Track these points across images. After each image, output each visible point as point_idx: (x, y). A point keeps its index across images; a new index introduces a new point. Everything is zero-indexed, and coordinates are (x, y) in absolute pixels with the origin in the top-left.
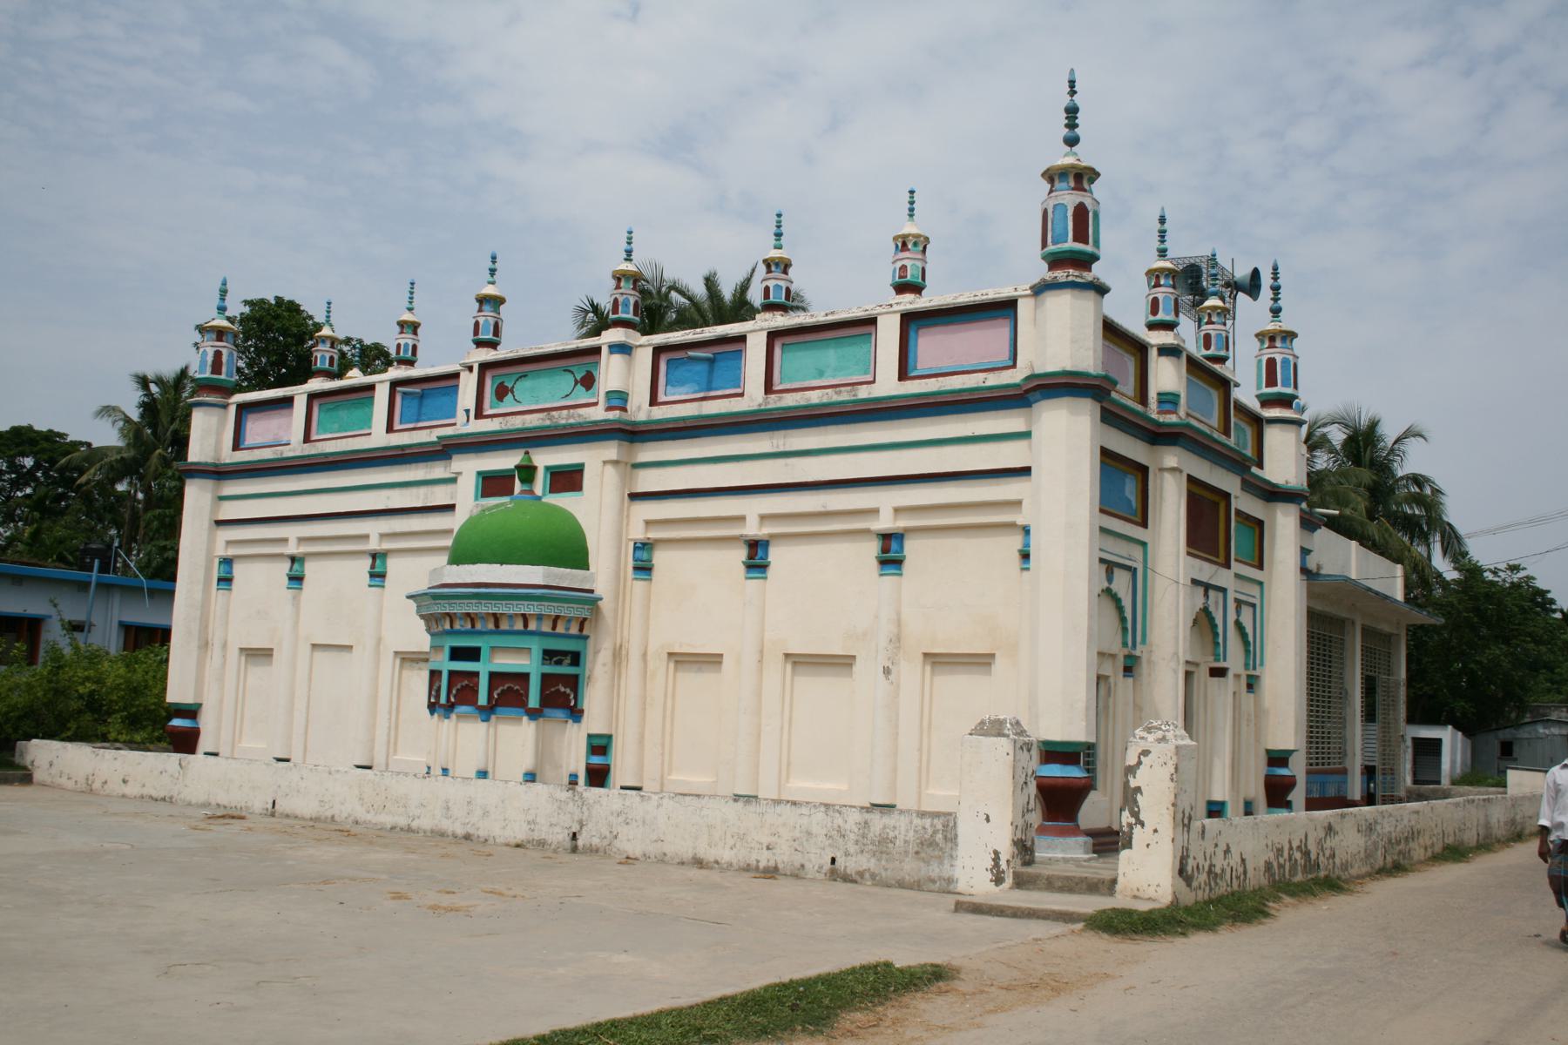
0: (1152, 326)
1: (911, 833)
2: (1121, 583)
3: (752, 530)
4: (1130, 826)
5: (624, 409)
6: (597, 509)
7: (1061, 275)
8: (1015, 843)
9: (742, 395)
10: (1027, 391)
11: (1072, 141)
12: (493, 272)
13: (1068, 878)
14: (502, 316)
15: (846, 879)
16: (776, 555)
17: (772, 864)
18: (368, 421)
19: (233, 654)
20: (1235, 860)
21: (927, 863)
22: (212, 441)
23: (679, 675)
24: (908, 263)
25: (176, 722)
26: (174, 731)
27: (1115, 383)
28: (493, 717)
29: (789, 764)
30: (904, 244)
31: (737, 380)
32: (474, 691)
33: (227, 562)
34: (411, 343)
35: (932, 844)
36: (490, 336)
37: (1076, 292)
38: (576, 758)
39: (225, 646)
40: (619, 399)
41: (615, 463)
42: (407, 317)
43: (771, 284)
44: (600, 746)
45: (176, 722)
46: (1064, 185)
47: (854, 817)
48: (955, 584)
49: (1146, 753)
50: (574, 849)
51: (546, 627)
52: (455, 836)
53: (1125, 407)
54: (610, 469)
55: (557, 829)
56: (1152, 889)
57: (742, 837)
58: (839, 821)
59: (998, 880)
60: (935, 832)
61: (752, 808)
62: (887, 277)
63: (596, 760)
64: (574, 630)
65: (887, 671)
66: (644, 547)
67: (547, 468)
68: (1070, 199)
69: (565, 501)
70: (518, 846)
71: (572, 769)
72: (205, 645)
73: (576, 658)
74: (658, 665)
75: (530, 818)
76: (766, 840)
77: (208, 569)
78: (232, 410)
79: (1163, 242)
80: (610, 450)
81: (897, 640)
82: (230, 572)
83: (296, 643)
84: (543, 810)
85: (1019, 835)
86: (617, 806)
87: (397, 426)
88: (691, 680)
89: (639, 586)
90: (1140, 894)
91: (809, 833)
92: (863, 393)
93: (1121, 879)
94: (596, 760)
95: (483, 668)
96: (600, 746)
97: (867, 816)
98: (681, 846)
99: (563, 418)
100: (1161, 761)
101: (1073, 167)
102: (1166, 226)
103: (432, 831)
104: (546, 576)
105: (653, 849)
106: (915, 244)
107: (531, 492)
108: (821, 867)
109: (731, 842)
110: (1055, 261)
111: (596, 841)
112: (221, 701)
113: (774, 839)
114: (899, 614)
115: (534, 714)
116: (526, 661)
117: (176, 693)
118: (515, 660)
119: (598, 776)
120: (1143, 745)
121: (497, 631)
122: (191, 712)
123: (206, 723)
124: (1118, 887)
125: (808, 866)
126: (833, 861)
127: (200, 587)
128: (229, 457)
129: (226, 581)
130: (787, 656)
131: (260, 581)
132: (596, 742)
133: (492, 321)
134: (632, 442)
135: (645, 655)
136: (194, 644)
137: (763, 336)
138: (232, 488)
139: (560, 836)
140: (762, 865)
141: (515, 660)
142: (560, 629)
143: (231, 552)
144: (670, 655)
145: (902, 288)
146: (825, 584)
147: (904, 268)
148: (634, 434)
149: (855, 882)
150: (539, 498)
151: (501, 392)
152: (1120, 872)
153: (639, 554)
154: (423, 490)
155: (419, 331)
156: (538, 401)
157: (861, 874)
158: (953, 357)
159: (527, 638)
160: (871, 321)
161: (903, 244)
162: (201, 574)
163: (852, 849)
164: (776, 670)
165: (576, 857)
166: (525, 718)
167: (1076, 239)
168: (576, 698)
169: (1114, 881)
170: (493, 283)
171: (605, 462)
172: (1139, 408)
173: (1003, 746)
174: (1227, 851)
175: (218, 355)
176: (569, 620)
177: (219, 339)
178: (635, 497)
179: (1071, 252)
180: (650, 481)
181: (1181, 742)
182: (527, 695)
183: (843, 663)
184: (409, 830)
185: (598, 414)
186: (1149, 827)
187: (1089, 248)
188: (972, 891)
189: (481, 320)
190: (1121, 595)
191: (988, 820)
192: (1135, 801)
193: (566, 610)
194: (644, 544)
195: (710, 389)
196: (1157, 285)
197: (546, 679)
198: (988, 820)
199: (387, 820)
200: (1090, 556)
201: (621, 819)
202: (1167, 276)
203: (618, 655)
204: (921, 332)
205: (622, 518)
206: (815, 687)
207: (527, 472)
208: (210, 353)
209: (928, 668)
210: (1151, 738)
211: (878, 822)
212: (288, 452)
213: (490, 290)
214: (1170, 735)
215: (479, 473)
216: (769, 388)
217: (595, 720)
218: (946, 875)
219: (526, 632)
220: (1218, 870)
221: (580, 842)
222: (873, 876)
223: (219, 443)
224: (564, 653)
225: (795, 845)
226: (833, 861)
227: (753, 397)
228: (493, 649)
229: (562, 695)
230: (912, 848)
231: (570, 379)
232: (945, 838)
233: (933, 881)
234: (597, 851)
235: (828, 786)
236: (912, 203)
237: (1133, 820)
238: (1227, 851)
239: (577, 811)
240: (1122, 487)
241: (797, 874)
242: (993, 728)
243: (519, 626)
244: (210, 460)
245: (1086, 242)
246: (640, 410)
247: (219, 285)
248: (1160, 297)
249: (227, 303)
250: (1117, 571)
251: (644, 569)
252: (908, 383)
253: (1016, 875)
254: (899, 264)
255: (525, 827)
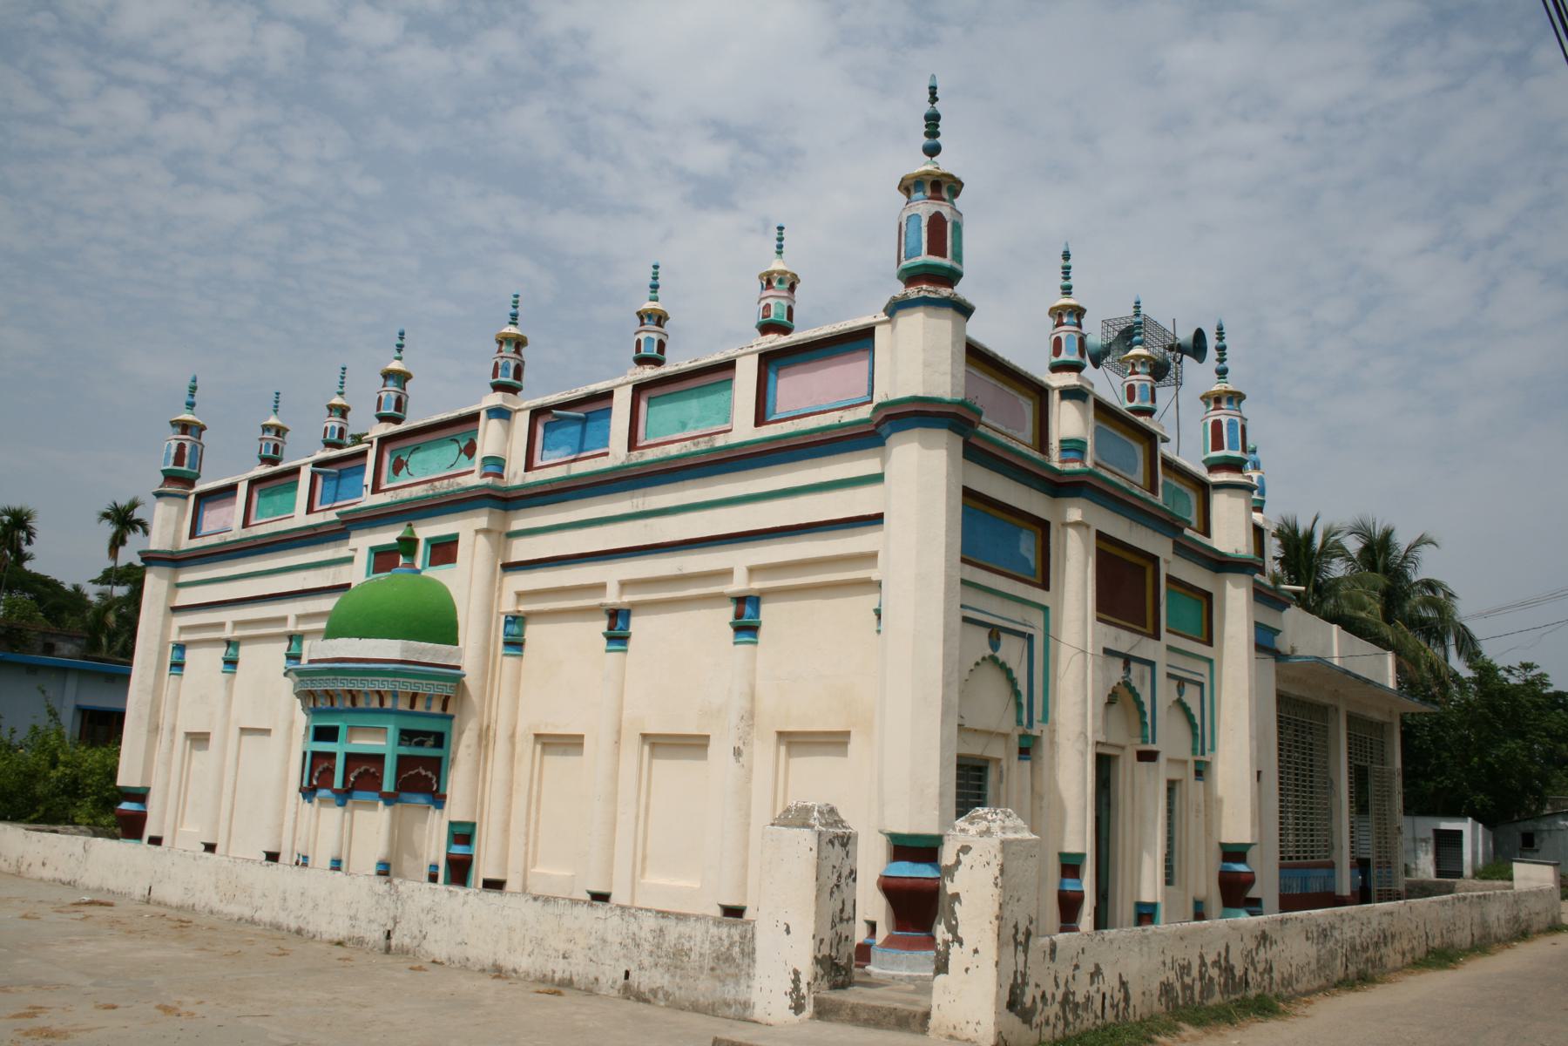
0: (1055, 368)
1: (707, 945)
2: (1011, 652)
3: (612, 598)
4: (946, 944)
5: (501, 476)
6: (467, 583)
7: (913, 293)
8: (817, 961)
9: (606, 454)
10: (877, 425)
11: (932, 151)
12: (400, 348)
13: (874, 1009)
14: (408, 391)
15: (640, 998)
16: (638, 626)
17: (567, 975)
18: (292, 506)
19: (180, 737)
20: (1109, 983)
21: (723, 982)
22: (171, 529)
23: (547, 758)
24: (771, 301)
25: (126, 806)
26: (122, 816)
27: (980, 413)
28: (350, 802)
29: (644, 858)
30: (769, 282)
31: (605, 441)
32: (330, 772)
33: (180, 647)
34: (337, 426)
35: (729, 959)
36: (392, 411)
37: (931, 310)
38: (434, 844)
39: (173, 730)
40: (496, 465)
41: (486, 532)
42: (337, 400)
43: (642, 336)
44: (462, 834)
45: (126, 806)
46: (920, 194)
47: (650, 922)
48: (814, 655)
49: (965, 849)
50: (388, 950)
51: (403, 705)
52: (289, 931)
53: (1020, 455)
54: (481, 539)
55: (375, 926)
56: (972, 1027)
57: (539, 942)
58: (634, 927)
59: (798, 1008)
60: (732, 945)
61: (550, 909)
62: (755, 317)
63: (459, 850)
64: (436, 708)
65: (737, 753)
66: (517, 620)
67: (428, 540)
68: (925, 208)
69: (440, 574)
70: (339, 943)
71: (432, 859)
72: (155, 729)
73: (439, 739)
74: (525, 746)
75: (352, 913)
76: (562, 947)
77: (162, 654)
78: (192, 499)
79: (1067, 278)
80: (481, 519)
81: (750, 717)
82: (182, 657)
83: (213, 723)
84: (341, 904)
85: (825, 950)
86: (427, 903)
87: (317, 507)
88: (556, 764)
89: (509, 662)
90: (957, 1033)
91: (604, 941)
92: (720, 441)
93: (934, 1013)
94: (459, 850)
95: (339, 748)
96: (462, 834)
97: (663, 922)
98: (483, 951)
99: (443, 487)
100: (984, 860)
101: (928, 174)
102: (1070, 262)
103: (271, 924)
104: (404, 651)
105: (457, 953)
106: (781, 282)
107: (413, 565)
108: (615, 982)
109: (529, 948)
110: (912, 277)
111: (407, 941)
112: (167, 785)
113: (570, 946)
114: (752, 688)
115: (390, 799)
116: (382, 742)
117: (127, 777)
118: (389, 744)
119: (459, 870)
120: (962, 840)
121: (354, 709)
122: (140, 796)
123: (153, 807)
124: (932, 1023)
125: (602, 980)
126: (627, 974)
127: (153, 672)
128: (186, 544)
129: (178, 666)
130: (645, 736)
131: (204, 662)
132: (458, 830)
133: (394, 396)
134: (506, 509)
135: (512, 736)
136: (144, 730)
137: (628, 390)
138: (186, 576)
139: (375, 935)
140: (558, 976)
141: (389, 744)
142: (420, 707)
143: (184, 638)
144: (537, 736)
145: (766, 328)
146: (683, 655)
147: (768, 307)
148: (505, 501)
149: (646, 1001)
150: (419, 572)
151: (398, 467)
152: (934, 1003)
153: (509, 628)
154: (331, 571)
155: (349, 415)
156: (432, 470)
157: (654, 992)
158: (814, 397)
159: (384, 717)
160: (730, 365)
161: (768, 281)
162: (154, 658)
163: (647, 961)
164: (632, 749)
165: (389, 959)
166: (381, 803)
167: (930, 252)
168: (438, 782)
169: (927, 1015)
170: (400, 359)
171: (477, 532)
172: (1037, 455)
173: (807, 838)
174: (1096, 973)
175: (181, 447)
176: (430, 698)
177: (184, 432)
178: (508, 567)
179: (926, 266)
180: (523, 550)
181: (1011, 836)
182: (381, 777)
183: (695, 745)
184: (252, 922)
185: (474, 480)
186: (968, 946)
187: (947, 262)
188: (771, 1020)
189: (384, 395)
190: (1011, 664)
191: (788, 931)
192: (953, 912)
193: (423, 687)
194: (515, 618)
195: (581, 450)
196: (1060, 324)
197: (403, 762)
198: (788, 931)
199: (235, 910)
200: (947, 612)
201: (430, 917)
202: (1070, 314)
203: (484, 737)
204: (782, 372)
205: (493, 590)
206: (669, 769)
207: (408, 545)
208: (174, 444)
209: (783, 749)
210: (973, 830)
211: (673, 930)
212: (229, 537)
213: (395, 365)
214: (995, 827)
215: (372, 549)
216: (632, 444)
217: (457, 808)
218: (741, 998)
219: (382, 711)
220: (1080, 998)
221: (393, 942)
222: (667, 995)
223: (178, 531)
224: (427, 734)
225: (590, 954)
226: (627, 974)
227: (617, 453)
228: (351, 729)
229: (421, 778)
230: (708, 963)
231: (454, 448)
232: (742, 952)
233: (729, 1005)
234: (408, 952)
235: (682, 883)
236: (780, 239)
237: (949, 937)
238: (1096, 973)
239: (392, 906)
240: (1000, 539)
241: (590, 991)
242: (797, 817)
243: (375, 704)
244: (168, 548)
245: (944, 256)
246: (516, 476)
247: (188, 382)
248: (1063, 335)
249: (196, 399)
250: (1004, 637)
251: (515, 644)
252: (764, 428)
253: (818, 1003)
254: (763, 303)
255: (348, 923)
